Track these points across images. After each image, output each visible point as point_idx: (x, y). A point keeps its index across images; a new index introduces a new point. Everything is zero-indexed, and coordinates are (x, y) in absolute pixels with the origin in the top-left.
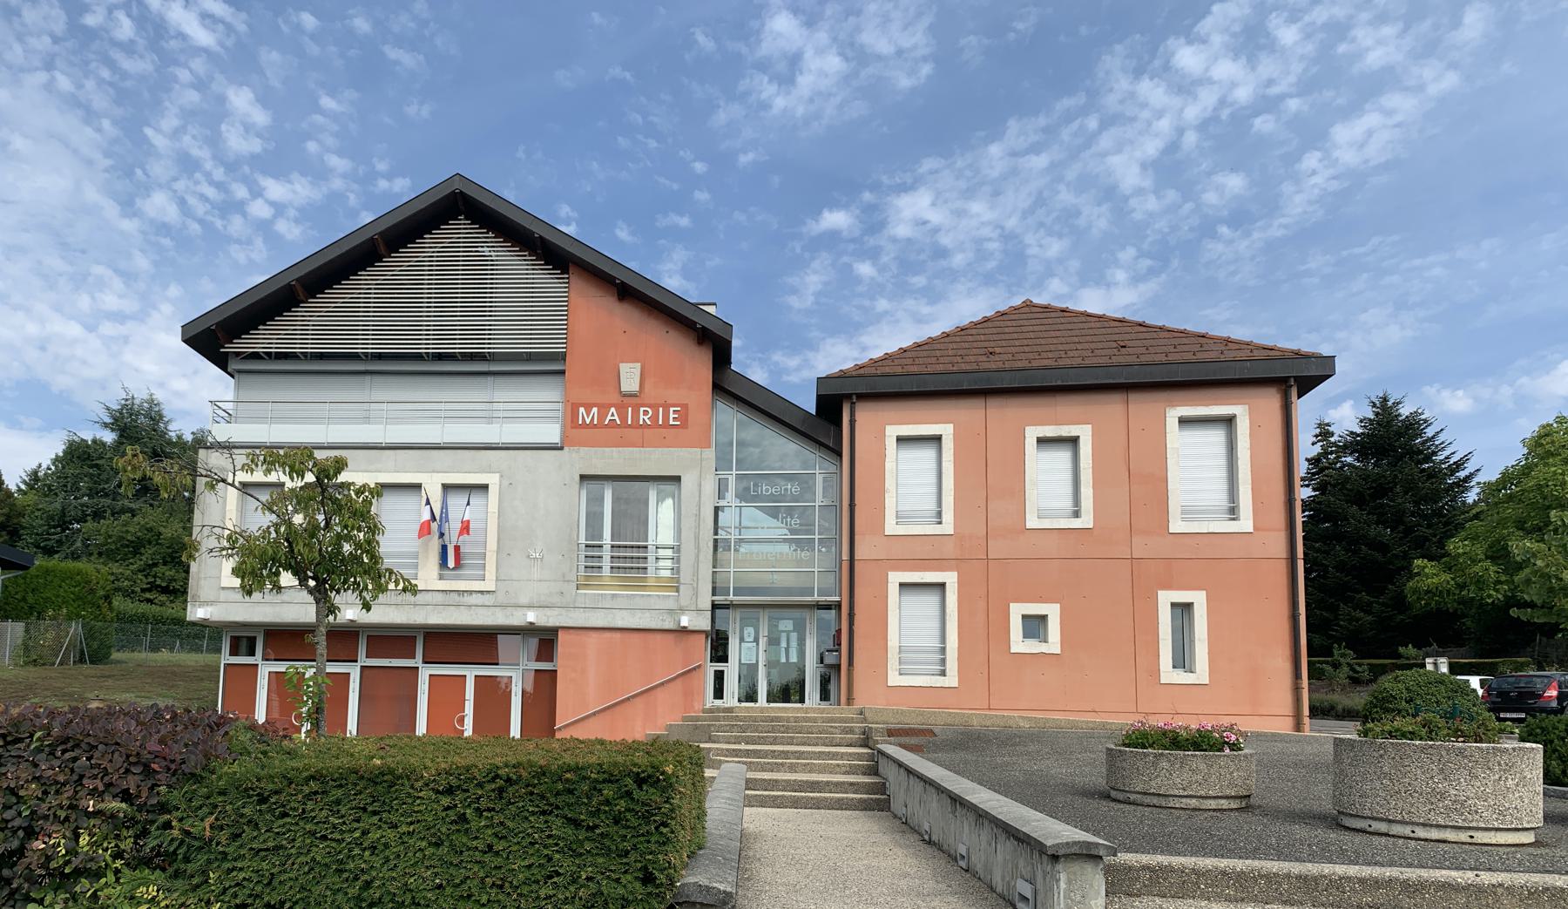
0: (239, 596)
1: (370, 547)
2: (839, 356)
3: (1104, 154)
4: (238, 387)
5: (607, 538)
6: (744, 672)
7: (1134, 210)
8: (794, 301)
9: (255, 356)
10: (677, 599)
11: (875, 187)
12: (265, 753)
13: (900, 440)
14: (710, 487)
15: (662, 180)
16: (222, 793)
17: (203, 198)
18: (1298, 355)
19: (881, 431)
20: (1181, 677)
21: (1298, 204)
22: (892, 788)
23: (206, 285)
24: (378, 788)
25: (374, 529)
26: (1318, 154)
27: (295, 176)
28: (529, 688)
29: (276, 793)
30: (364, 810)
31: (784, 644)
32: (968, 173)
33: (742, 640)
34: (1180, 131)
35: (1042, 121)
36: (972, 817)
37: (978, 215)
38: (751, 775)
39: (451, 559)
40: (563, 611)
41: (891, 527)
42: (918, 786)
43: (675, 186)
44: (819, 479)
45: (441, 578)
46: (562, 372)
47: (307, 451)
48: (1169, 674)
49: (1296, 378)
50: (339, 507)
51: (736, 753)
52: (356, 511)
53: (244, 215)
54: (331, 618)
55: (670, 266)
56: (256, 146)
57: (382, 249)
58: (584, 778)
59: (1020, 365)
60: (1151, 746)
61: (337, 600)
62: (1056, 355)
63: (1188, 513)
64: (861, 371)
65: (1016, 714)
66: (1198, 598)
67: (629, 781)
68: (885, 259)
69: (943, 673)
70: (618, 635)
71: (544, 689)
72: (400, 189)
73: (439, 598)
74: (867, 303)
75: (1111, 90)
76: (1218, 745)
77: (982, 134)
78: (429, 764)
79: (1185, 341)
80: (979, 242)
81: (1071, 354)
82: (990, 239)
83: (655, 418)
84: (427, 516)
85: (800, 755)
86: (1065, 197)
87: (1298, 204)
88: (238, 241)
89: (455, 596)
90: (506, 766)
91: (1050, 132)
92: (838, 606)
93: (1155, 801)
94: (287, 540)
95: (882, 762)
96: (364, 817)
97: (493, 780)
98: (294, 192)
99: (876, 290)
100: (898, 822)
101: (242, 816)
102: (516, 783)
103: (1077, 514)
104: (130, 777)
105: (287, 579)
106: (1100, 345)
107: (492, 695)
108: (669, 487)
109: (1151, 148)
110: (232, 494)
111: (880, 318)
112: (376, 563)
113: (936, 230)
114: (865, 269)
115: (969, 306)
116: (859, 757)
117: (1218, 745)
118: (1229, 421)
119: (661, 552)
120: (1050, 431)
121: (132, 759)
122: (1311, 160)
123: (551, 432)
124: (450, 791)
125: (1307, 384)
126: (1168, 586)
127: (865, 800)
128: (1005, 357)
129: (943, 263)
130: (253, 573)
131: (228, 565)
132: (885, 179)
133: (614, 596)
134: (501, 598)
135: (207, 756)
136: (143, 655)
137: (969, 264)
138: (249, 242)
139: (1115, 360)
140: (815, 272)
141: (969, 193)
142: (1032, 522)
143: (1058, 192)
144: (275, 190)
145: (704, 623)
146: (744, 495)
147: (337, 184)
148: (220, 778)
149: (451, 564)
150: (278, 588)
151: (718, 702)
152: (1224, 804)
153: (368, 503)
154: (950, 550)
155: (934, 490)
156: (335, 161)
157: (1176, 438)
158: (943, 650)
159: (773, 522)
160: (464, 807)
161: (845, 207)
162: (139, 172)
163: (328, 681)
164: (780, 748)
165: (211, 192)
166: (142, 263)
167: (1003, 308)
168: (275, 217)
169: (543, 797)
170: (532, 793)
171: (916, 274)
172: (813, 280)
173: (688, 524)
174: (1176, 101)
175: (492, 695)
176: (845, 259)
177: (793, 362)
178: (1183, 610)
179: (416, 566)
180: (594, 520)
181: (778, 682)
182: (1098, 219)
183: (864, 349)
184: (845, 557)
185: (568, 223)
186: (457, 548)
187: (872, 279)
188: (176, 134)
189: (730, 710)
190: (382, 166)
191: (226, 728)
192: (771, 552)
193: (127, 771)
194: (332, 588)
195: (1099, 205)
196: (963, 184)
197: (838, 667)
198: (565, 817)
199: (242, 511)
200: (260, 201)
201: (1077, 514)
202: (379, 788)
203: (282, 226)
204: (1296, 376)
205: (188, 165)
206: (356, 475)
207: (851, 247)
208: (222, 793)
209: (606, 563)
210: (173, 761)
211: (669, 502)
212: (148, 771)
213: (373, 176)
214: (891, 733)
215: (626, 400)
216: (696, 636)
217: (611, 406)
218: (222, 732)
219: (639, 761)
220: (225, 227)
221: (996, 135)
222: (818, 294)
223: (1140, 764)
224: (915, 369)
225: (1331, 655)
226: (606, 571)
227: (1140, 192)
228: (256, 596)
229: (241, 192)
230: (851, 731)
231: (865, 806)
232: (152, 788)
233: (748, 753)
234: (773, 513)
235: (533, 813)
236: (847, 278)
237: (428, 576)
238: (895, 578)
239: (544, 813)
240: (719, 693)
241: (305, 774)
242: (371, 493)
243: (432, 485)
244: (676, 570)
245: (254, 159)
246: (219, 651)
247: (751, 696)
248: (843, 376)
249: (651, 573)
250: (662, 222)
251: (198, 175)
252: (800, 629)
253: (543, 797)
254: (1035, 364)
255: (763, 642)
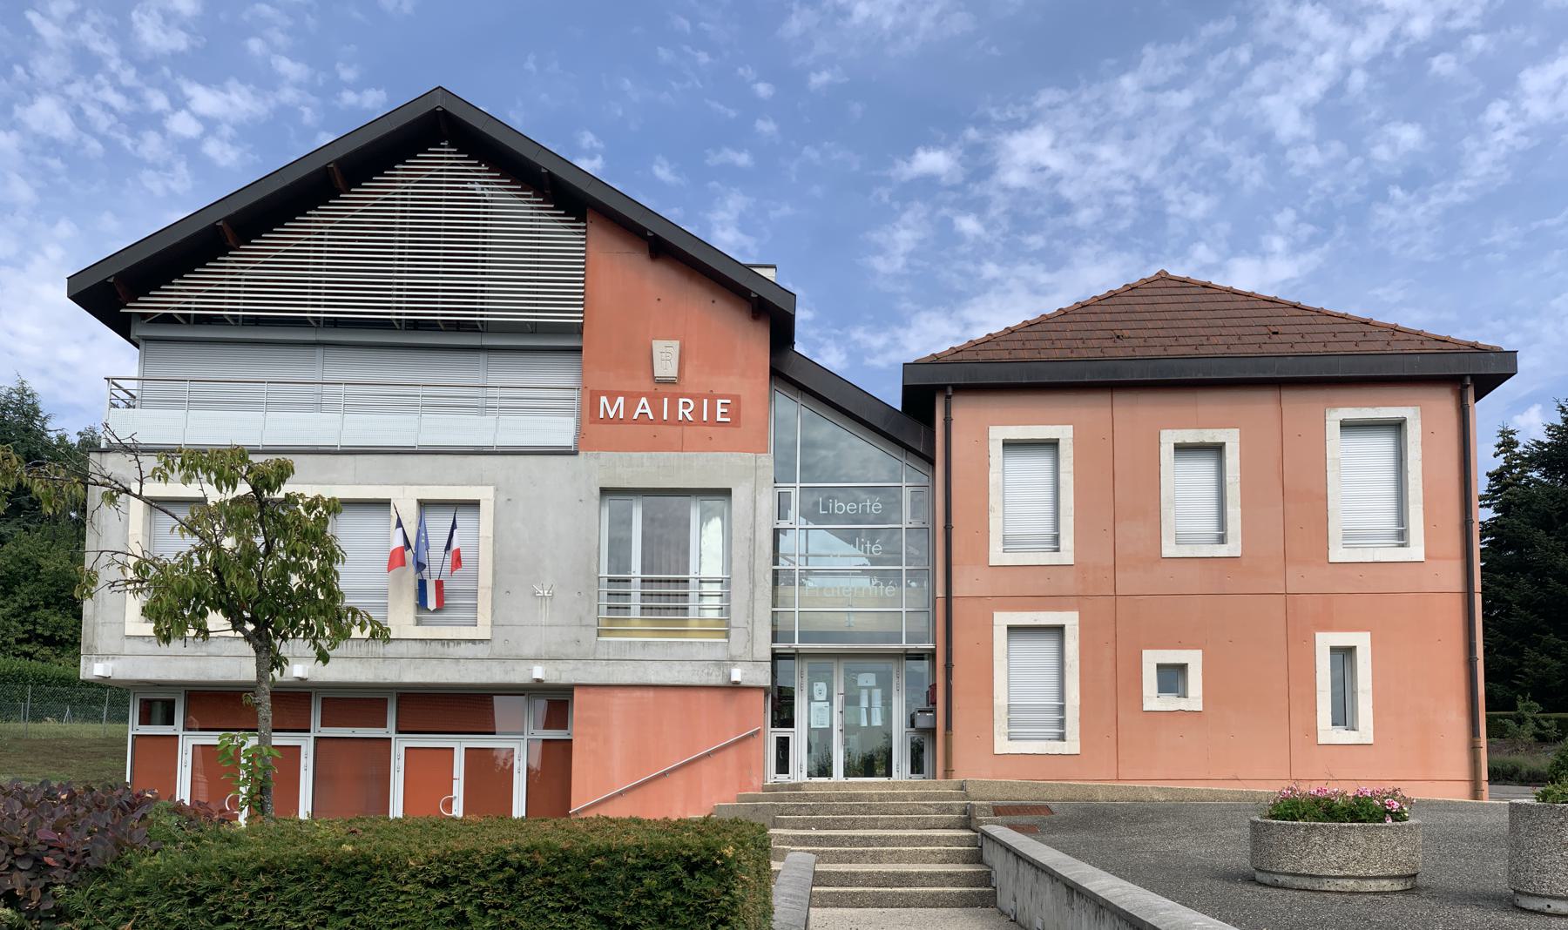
0: (152, 647)
1: (326, 579)
2: (933, 335)
3: (1258, 94)
4: (144, 360)
5: (636, 571)
6: (815, 741)
7: (1292, 164)
8: (879, 264)
9: (168, 319)
10: (727, 646)
11: (982, 122)
12: (197, 840)
13: (1008, 445)
14: (767, 502)
15: (715, 105)
16: (142, 893)
17: (108, 108)
18: (1476, 349)
19: (983, 432)
20: (1342, 736)
21: (1482, 164)
22: (999, 878)
23: (109, 223)
24: (353, 879)
25: (331, 555)
26: (1505, 105)
27: (232, 83)
28: (536, 764)
29: (214, 890)
30: (332, 909)
31: (864, 704)
32: (1096, 110)
33: (811, 698)
34: (1347, 70)
35: (1185, 49)
36: (1091, 909)
37: (1108, 162)
38: (820, 868)
39: (430, 597)
40: (580, 664)
41: (997, 556)
42: (1028, 874)
43: (732, 114)
44: (906, 495)
45: (419, 622)
46: (579, 350)
47: (241, 454)
48: (1329, 733)
49: (1473, 377)
50: (283, 528)
51: (804, 841)
52: (308, 532)
53: (162, 131)
54: (276, 672)
55: (721, 215)
56: (179, 41)
57: (339, 182)
58: (619, 864)
59: (1153, 352)
60: (1302, 817)
61: (284, 649)
62: (1197, 341)
63: (1350, 537)
64: (959, 357)
65: (1149, 785)
66: (1361, 641)
67: (677, 867)
68: (993, 213)
69: (1062, 737)
70: (651, 694)
71: (556, 762)
72: (370, 102)
73: (417, 649)
74: (971, 267)
75: (1266, 15)
76: (1379, 815)
77: (1112, 62)
78: (416, 849)
79: (1346, 328)
80: (1109, 194)
81: (1214, 340)
82: (1122, 193)
83: (698, 412)
84: (398, 542)
85: (884, 841)
86: (1212, 144)
87: (1482, 164)
88: (154, 166)
89: (438, 646)
90: (517, 850)
91: (1194, 64)
92: (932, 655)
93: (1307, 883)
94: (216, 570)
95: (987, 846)
96: (332, 919)
97: (500, 868)
98: (231, 104)
99: (982, 251)
100: (1005, 920)
101: (168, 922)
102: (530, 871)
103: (1222, 540)
104: (16, 875)
105: (216, 621)
106: (1247, 331)
107: (488, 774)
108: (716, 504)
109: (1313, 89)
110: (137, 508)
111: (987, 286)
112: (335, 600)
113: (1056, 179)
114: (968, 225)
115: (1096, 276)
116: (959, 841)
117: (1379, 815)
118: (1398, 426)
119: (706, 588)
120: (1190, 436)
121: (17, 851)
122: (1497, 112)
123: (561, 430)
124: (444, 883)
125: (1486, 384)
126: (1328, 627)
127: (961, 894)
128: (1135, 342)
129: (1067, 220)
130: (173, 614)
131: (134, 605)
132: (994, 113)
133: (645, 644)
134: (498, 648)
135: (119, 846)
136: (21, 726)
137: (1097, 223)
138: (169, 167)
139: (1267, 349)
140: (906, 227)
141: (1097, 134)
142: (1169, 549)
143: (1204, 138)
144: (205, 100)
145: (763, 677)
146: (809, 514)
147: (288, 95)
148: (137, 874)
149: (432, 604)
150: (204, 633)
151: (782, 778)
152: (1386, 885)
153: (322, 521)
154: (1069, 584)
155: (1049, 508)
156: (285, 66)
157: (1339, 448)
158: (1062, 709)
159: (849, 549)
160: (463, 904)
161: (945, 146)
162: (19, 70)
163: (276, 753)
164: (861, 833)
165: (116, 100)
166: (22, 191)
167: (1134, 279)
168: (204, 135)
169: (565, 889)
170: (551, 885)
171: (1032, 232)
172: (905, 236)
173: (740, 550)
174: (1343, 33)
175: (488, 774)
176: (945, 211)
177: (878, 341)
178: (1344, 655)
179: (385, 607)
180: (619, 549)
181: (859, 752)
182: (1251, 173)
183: (967, 326)
184: (940, 593)
185: (590, 161)
186: (439, 584)
187: (977, 237)
188: (71, 21)
189: (797, 787)
190: (348, 75)
191: (143, 810)
192: (847, 587)
193: (11, 867)
194: (277, 632)
195: (1252, 155)
196: (1089, 123)
197: (932, 732)
198: (595, 914)
199: (150, 534)
200: (183, 114)
201: (1222, 540)
202: (351, 881)
203: (212, 148)
204: (1473, 374)
205: (86, 63)
206: (304, 485)
207: (952, 196)
208: (142, 893)
209: (635, 602)
210: (74, 853)
211: (716, 524)
212: (40, 867)
213: (336, 86)
214: (998, 811)
215: (661, 388)
216: (748, 696)
217: (641, 395)
218: (138, 815)
219: (690, 842)
220: (135, 147)
221: (1129, 64)
222: (911, 255)
223: (1289, 839)
224: (1025, 355)
225: (1515, 708)
226: (635, 613)
227: (1299, 142)
228: (176, 645)
229: (159, 102)
230: (949, 810)
231: (965, 902)
232: (45, 890)
233: (820, 840)
234: (850, 537)
235: (553, 910)
236: (947, 236)
237: (402, 619)
238: (1003, 619)
239: (567, 909)
240: (783, 766)
241: (252, 866)
242: (326, 507)
243: (405, 502)
244: (725, 610)
245: (175, 58)
246: (125, 719)
247: (824, 770)
248: (935, 361)
249: (692, 614)
250: (714, 159)
251: (100, 77)
252: (885, 684)
253: (565, 889)
254: (1172, 352)
255: (838, 701)
